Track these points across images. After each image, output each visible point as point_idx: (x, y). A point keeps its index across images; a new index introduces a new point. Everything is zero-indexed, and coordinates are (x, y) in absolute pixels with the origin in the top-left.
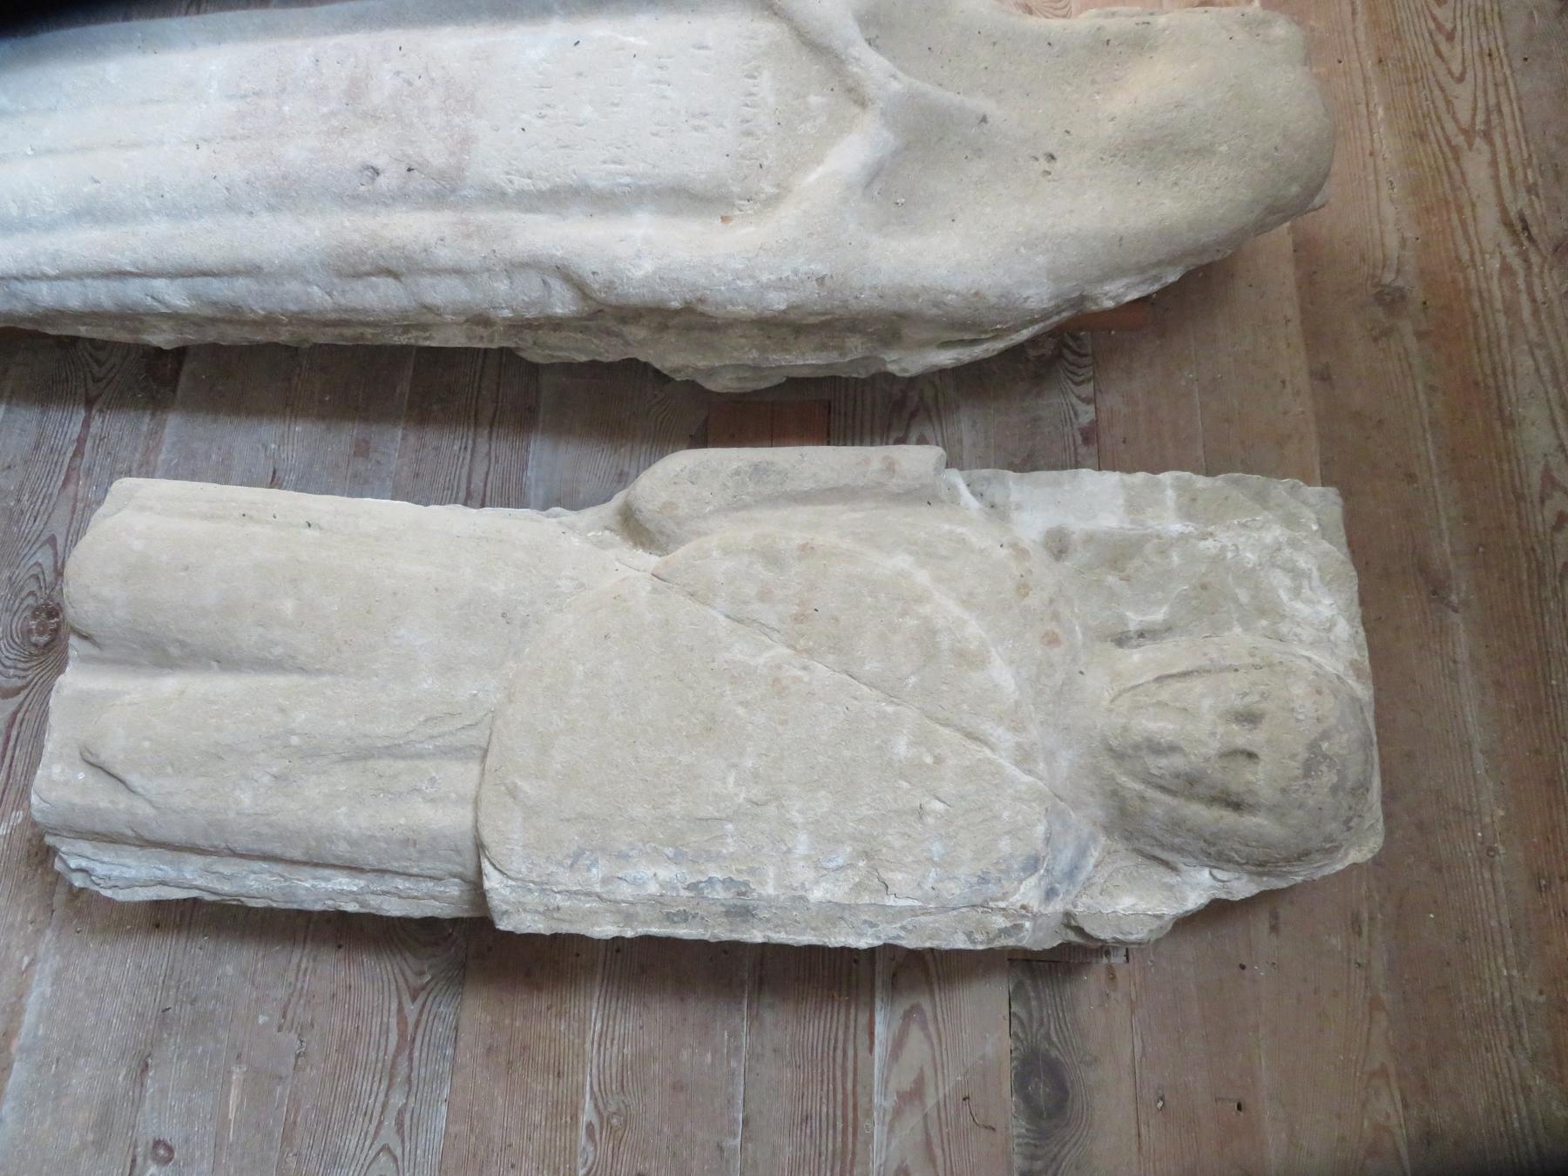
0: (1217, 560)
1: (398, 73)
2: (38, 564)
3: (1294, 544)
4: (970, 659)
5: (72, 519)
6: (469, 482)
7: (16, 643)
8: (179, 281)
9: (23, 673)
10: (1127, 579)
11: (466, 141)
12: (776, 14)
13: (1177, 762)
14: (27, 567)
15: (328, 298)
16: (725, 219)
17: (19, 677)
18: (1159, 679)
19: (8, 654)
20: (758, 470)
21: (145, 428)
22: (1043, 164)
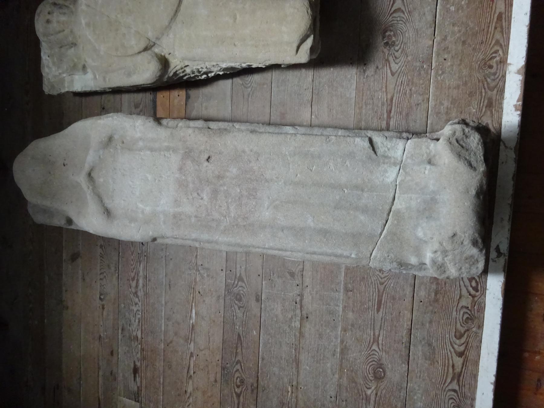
0: (59, 68)
1: (202, 199)
2: (397, 64)
3: (48, 74)
4: (88, 25)
5: (386, 84)
6: (248, 105)
7: (399, 30)
8: (284, 132)
9: (394, 19)
10: (73, 61)
11: (181, 169)
12: (107, 210)
13: (61, 11)
14: (401, 62)
15: (235, 125)
16: (123, 143)
17: (395, 17)
18: (64, 31)
19: (401, 25)
20: (129, 75)
21: (363, 123)
22: (65, 163)
